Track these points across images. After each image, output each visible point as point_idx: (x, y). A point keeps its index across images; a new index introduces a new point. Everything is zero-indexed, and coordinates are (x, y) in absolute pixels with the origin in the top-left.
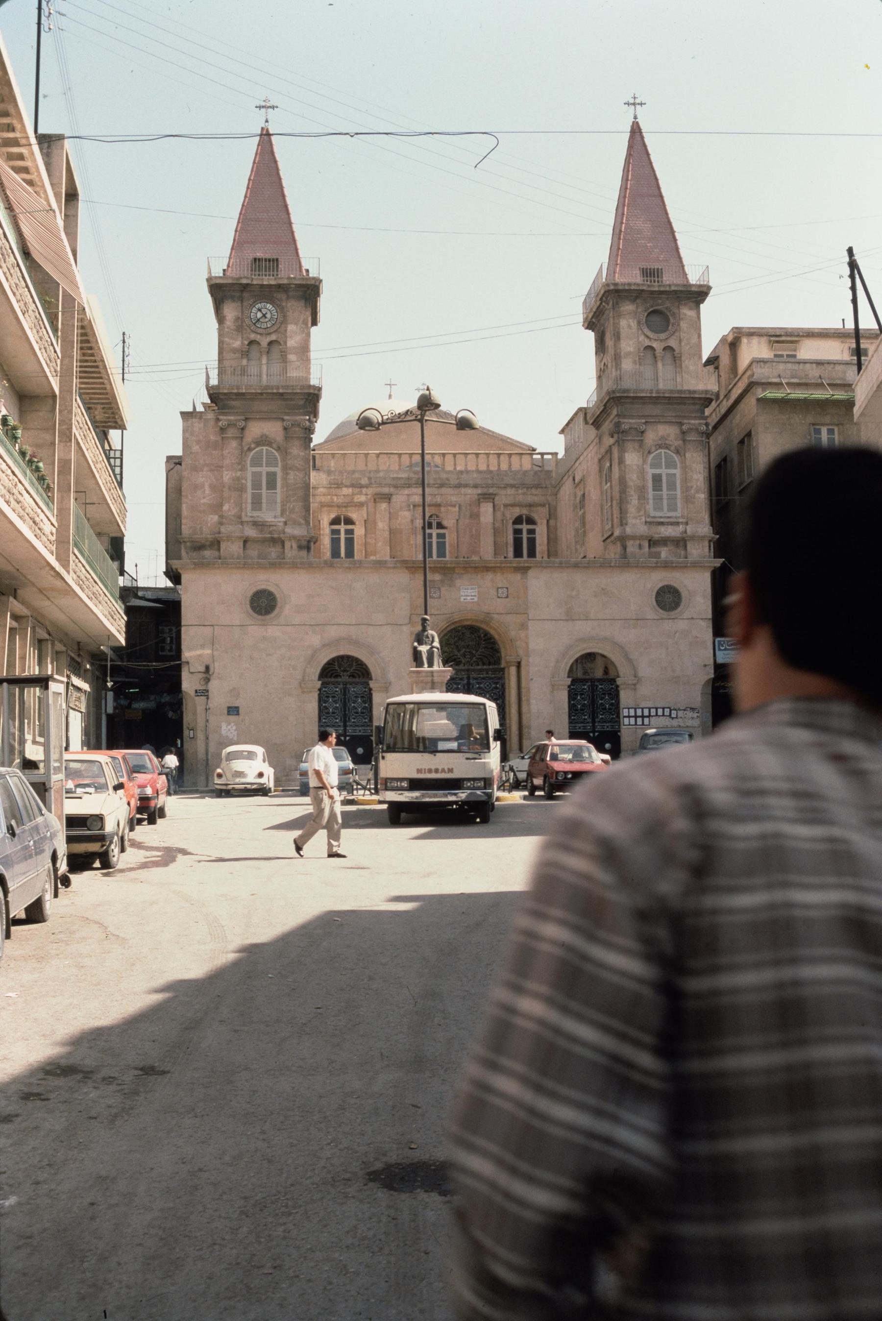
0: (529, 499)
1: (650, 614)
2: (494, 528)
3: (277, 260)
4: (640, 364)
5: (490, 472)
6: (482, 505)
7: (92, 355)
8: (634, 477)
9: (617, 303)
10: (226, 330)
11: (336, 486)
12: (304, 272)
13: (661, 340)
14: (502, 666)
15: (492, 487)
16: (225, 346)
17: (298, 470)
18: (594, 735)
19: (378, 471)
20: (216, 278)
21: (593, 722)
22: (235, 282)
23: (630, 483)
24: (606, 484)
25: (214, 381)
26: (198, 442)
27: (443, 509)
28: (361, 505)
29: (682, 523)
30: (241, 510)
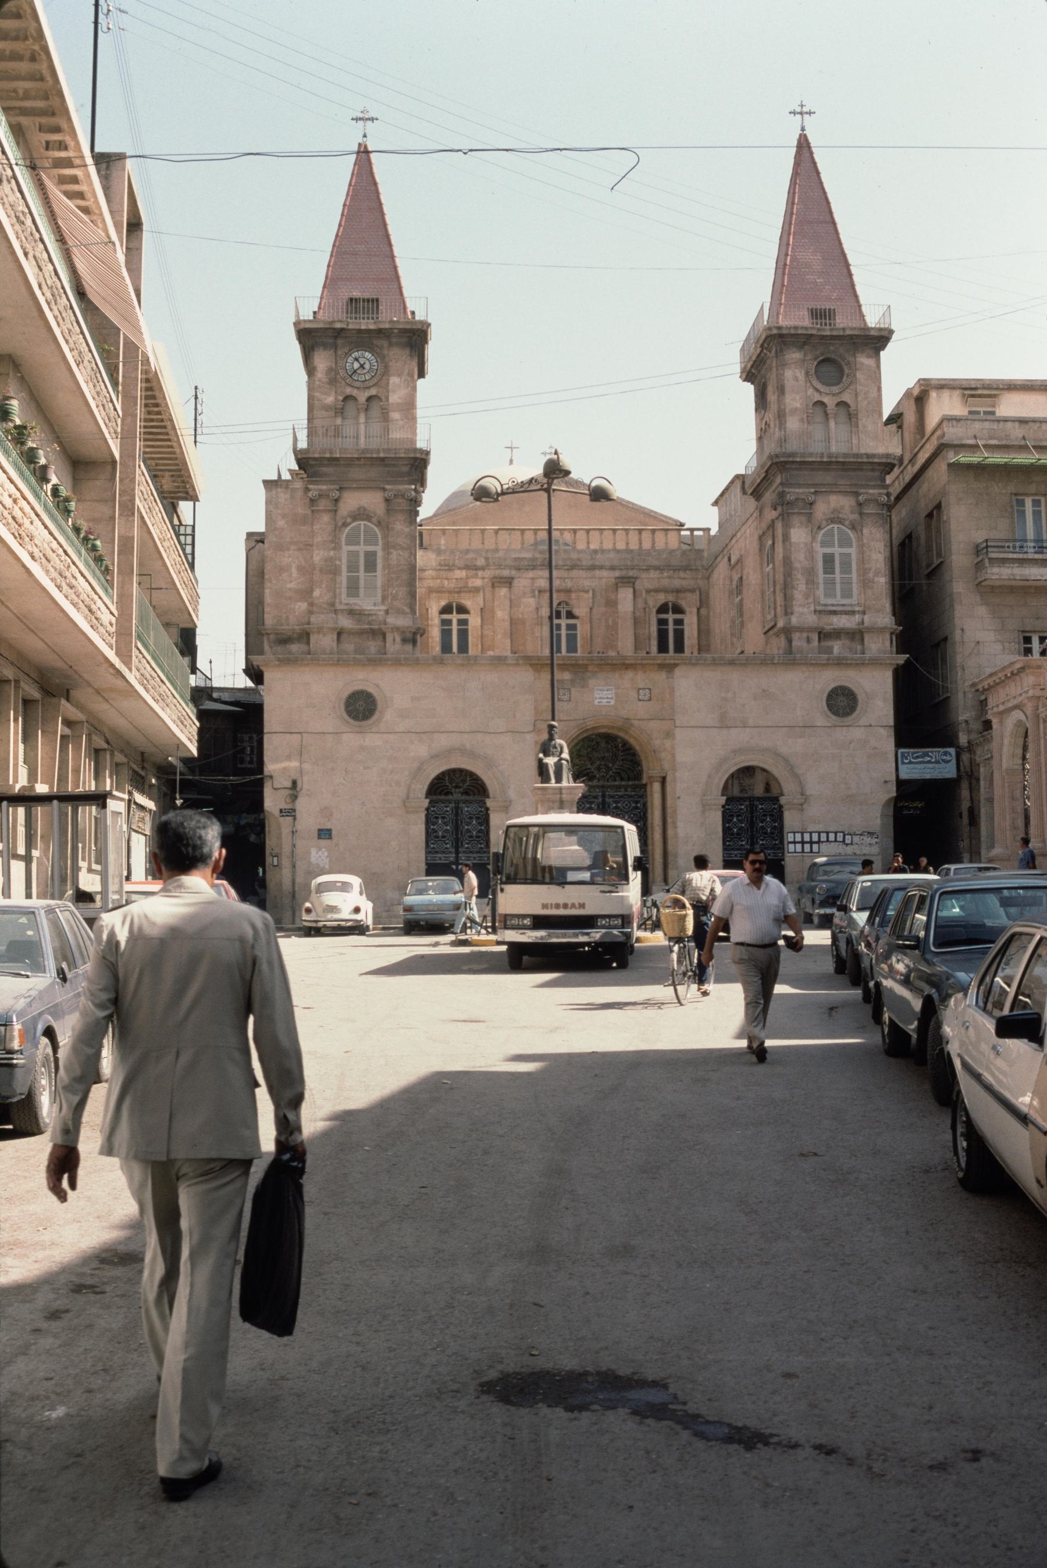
0: (677, 583)
2: (635, 619)
3: (377, 300)
4: (809, 423)
7: (159, 413)
8: (801, 556)
9: (781, 350)
10: (317, 383)
11: (446, 568)
12: (409, 313)
13: (834, 395)
14: (644, 781)
15: (632, 569)
16: (316, 402)
17: (403, 549)
19: (496, 550)
20: (305, 321)
22: (327, 326)
23: (797, 565)
24: (768, 565)
25: (303, 444)
26: (284, 516)
27: (573, 596)
28: (476, 590)
29: (858, 612)
30: (334, 596)
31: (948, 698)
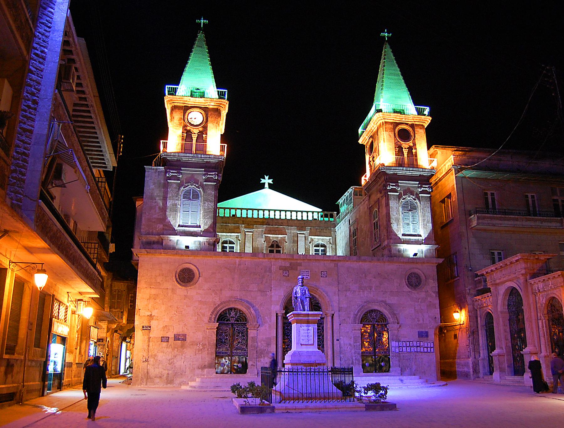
1: (407, 289)
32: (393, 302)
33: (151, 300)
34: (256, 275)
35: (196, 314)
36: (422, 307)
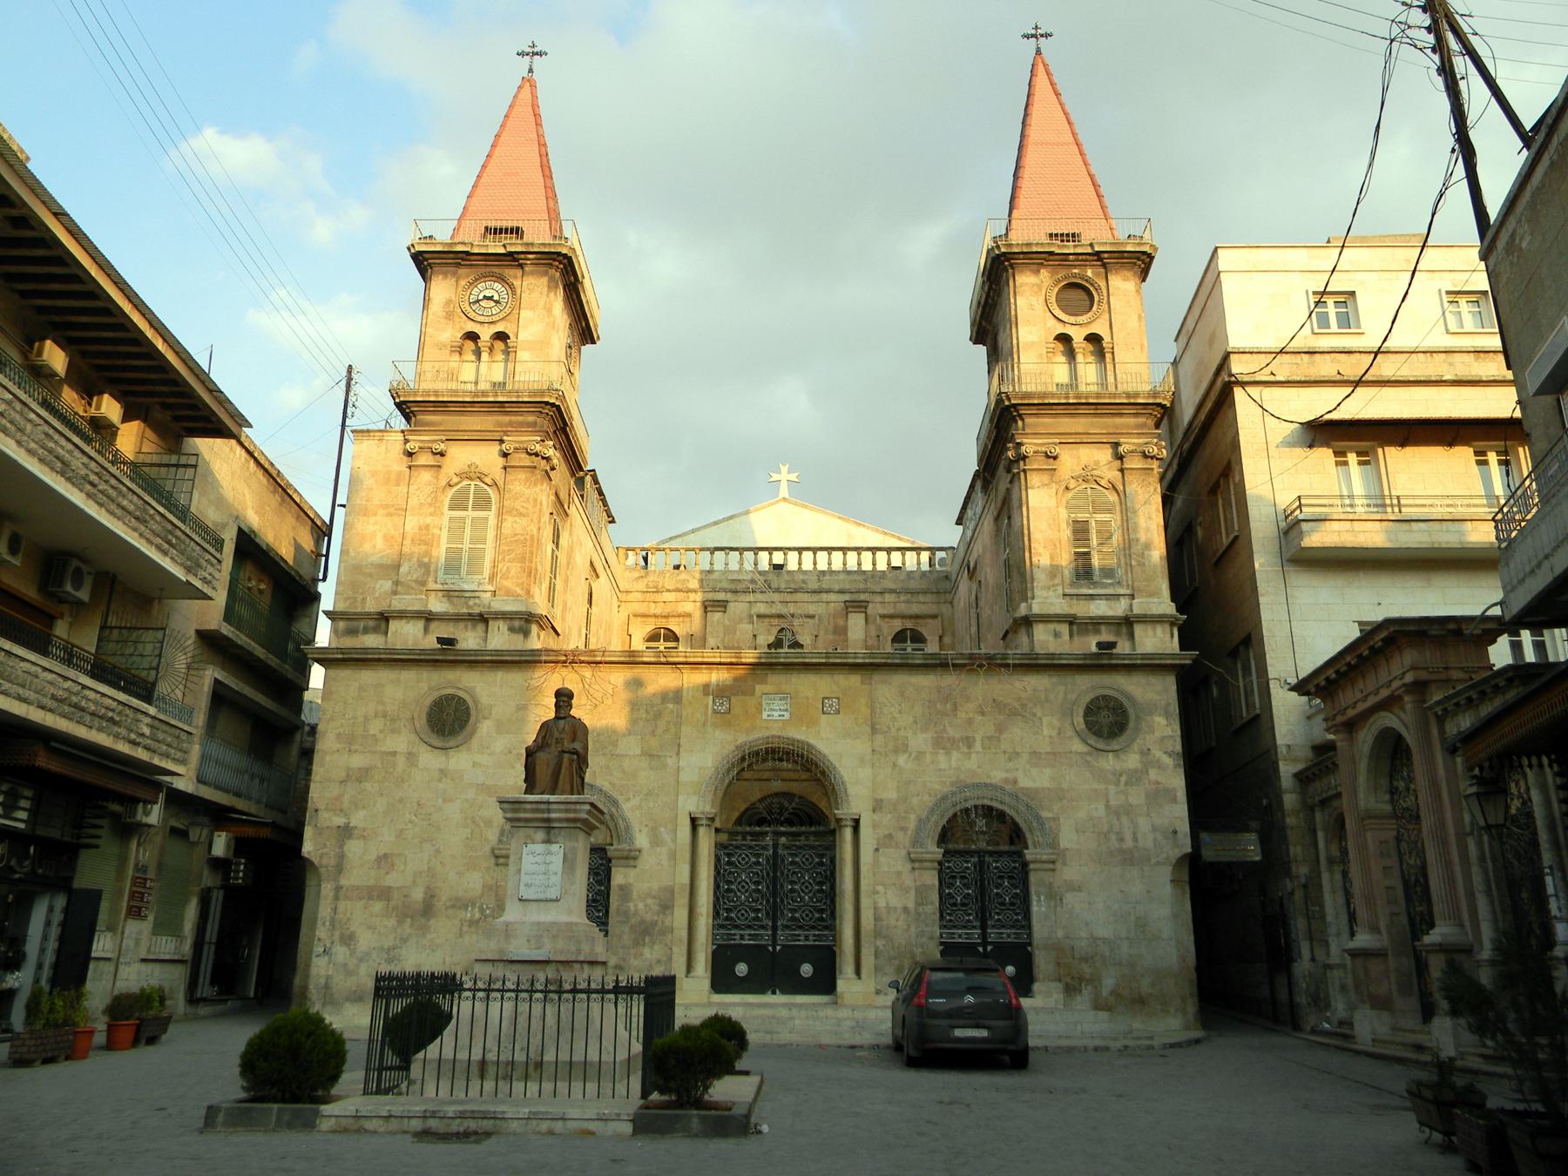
0: (915, 609)
1: (1078, 746)
5: (860, 572)
6: (850, 615)
8: (1044, 526)
15: (864, 592)
18: (985, 949)
21: (984, 927)
31: (1257, 717)
32: (1038, 784)
33: (349, 784)
34: (639, 710)
35: (469, 821)
36: (1130, 798)
